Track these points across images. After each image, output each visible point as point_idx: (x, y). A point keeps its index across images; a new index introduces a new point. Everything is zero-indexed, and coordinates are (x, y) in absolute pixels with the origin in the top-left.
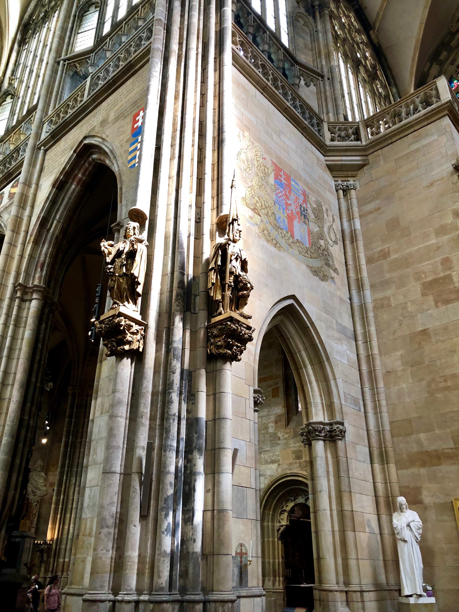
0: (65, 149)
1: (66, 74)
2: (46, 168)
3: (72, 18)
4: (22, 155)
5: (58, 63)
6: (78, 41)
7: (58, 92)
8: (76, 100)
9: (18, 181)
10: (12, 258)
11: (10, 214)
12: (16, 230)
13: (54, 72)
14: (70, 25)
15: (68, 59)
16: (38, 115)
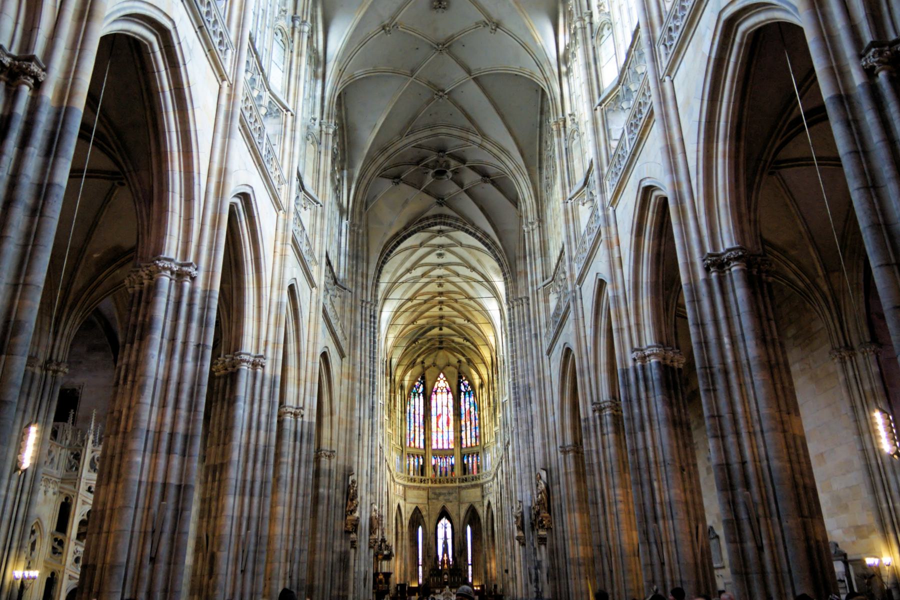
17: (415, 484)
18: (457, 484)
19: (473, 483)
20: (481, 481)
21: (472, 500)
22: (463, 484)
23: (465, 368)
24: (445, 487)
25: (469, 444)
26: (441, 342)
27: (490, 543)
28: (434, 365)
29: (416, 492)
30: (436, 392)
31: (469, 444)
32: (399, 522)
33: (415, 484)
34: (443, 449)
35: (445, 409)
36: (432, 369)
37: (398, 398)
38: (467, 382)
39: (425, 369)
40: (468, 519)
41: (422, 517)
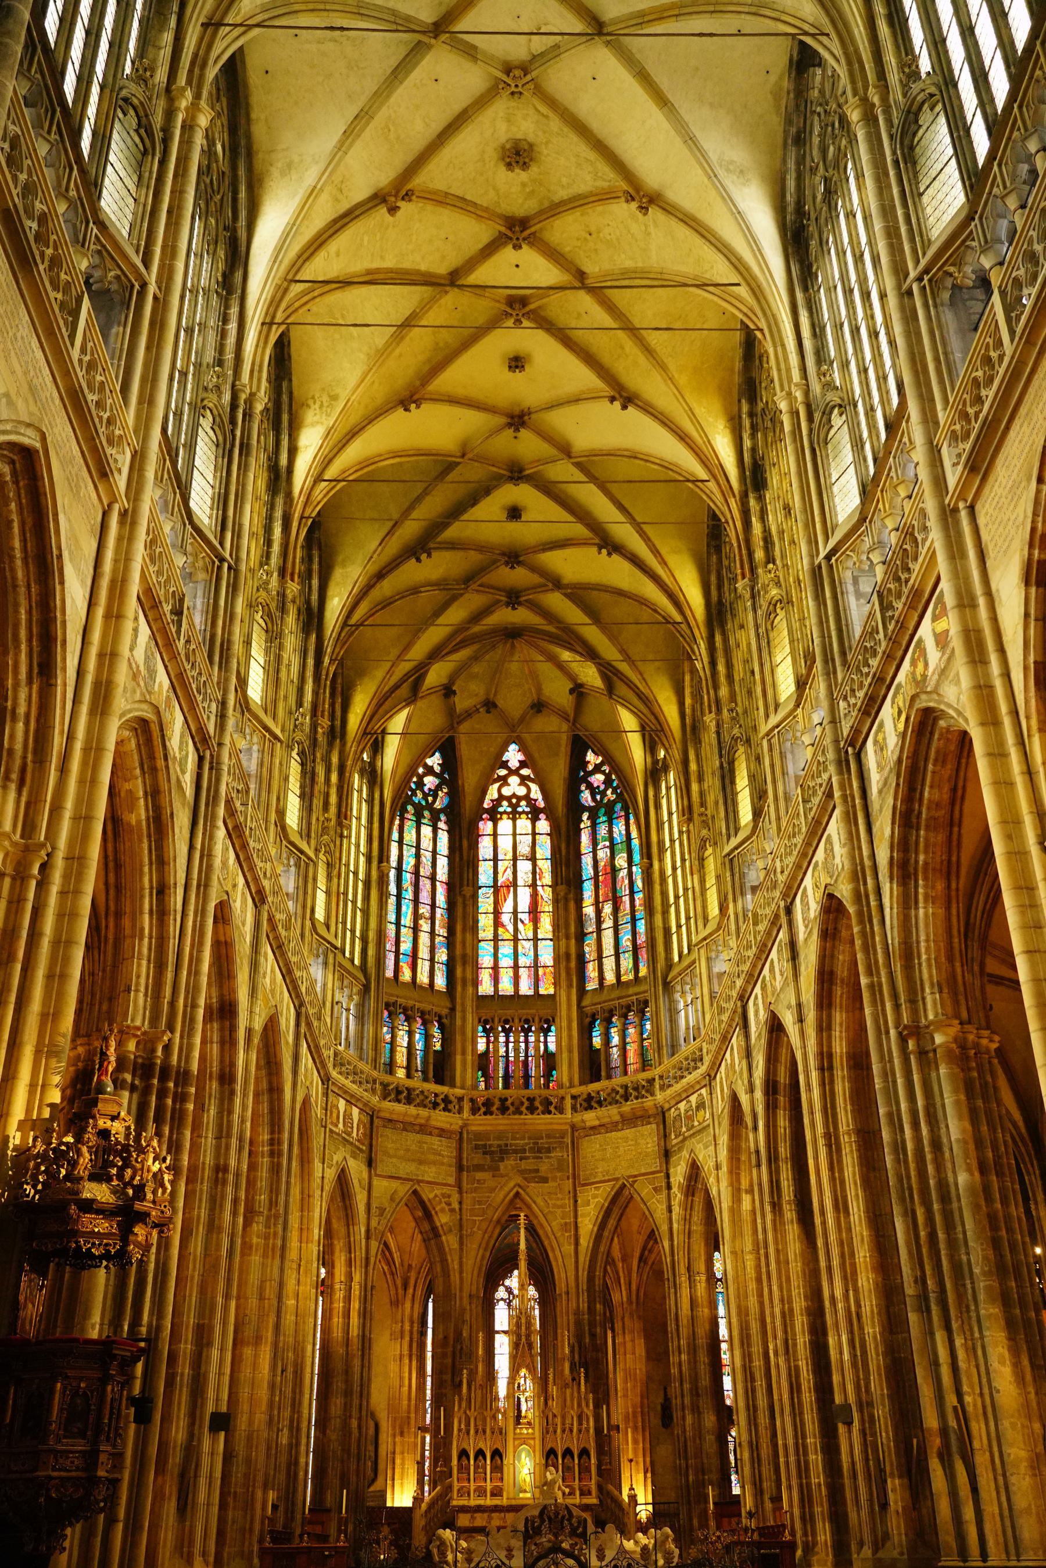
0: (1016, 485)
1: (936, 306)
2: (991, 547)
3: (892, 173)
4: (924, 540)
5: (910, 293)
6: (929, 210)
7: (937, 359)
8: (987, 361)
9: (941, 600)
10: (1010, 784)
11: (958, 682)
12: (991, 720)
13: (909, 318)
14: (895, 191)
15: (926, 271)
16: (915, 428)
17: (412, 1110)
20: (660, 1096)
21: (624, 1171)
23: (592, 720)
25: (610, 977)
26: (514, 598)
28: (490, 705)
29: (412, 1139)
30: (494, 815)
31: (610, 977)
34: (516, 996)
35: (524, 867)
36: (484, 722)
37: (359, 808)
38: (601, 777)
39: (454, 719)
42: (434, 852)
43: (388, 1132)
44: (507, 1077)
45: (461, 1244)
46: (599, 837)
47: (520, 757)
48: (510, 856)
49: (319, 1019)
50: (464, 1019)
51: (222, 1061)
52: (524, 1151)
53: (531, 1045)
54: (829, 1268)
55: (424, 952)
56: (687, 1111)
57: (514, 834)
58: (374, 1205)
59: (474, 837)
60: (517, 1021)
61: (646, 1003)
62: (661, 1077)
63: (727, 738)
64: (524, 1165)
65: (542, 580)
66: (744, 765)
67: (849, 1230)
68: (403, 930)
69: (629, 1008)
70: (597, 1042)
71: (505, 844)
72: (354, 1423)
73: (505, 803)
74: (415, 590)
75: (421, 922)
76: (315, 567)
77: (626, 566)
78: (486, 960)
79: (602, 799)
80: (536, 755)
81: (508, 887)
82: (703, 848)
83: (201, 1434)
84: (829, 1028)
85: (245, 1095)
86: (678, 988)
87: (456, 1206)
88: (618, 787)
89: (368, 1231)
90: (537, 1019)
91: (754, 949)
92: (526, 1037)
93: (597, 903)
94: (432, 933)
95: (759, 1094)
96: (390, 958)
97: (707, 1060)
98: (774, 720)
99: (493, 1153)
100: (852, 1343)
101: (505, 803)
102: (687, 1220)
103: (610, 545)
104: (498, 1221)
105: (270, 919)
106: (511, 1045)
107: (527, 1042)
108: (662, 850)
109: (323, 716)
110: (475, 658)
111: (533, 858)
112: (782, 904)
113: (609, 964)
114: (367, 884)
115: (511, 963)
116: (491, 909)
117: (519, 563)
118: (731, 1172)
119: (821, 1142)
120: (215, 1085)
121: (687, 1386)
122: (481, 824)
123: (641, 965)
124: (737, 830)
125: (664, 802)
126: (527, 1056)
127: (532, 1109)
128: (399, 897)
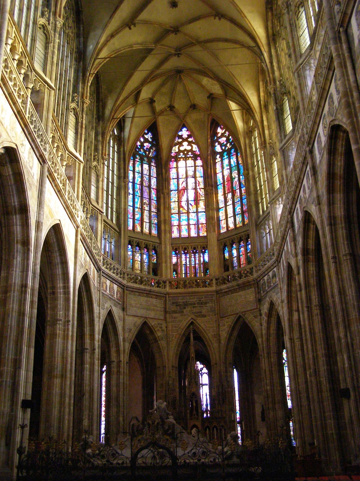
17: (142, 287)
18: (214, 288)
19: (241, 281)
20: (255, 275)
22: (224, 286)
24: (194, 292)
25: (231, 226)
26: (178, 52)
27: (276, 376)
28: (171, 108)
29: (143, 300)
30: (177, 159)
32: (113, 343)
33: (142, 287)
34: (189, 237)
35: (191, 181)
38: (224, 139)
40: (232, 344)
41: (156, 340)
42: (150, 176)
43: (132, 296)
44: (186, 273)
45: (168, 344)
46: (224, 165)
47: (187, 133)
48: (184, 176)
49: (91, 239)
50: (166, 247)
51: (23, 235)
52: (195, 304)
53: (197, 258)
54: (337, 323)
55: (146, 219)
56: (268, 280)
57: (186, 167)
58: (126, 328)
59: (168, 170)
60: (190, 248)
61: (248, 237)
62: (256, 267)
63: (278, 93)
64: (195, 310)
65: (191, 40)
66: (288, 105)
67: (346, 303)
68: (136, 210)
69: (240, 240)
70: (227, 255)
71: (182, 172)
72: (121, 419)
73: (182, 154)
74: (131, 46)
75: (144, 206)
76: (82, 32)
77: (228, 24)
78: (175, 222)
79: (225, 148)
80: (194, 130)
81: (184, 190)
82: (271, 159)
83: (17, 409)
84: (333, 204)
85: (36, 253)
86: (263, 227)
87: (164, 328)
88: (232, 141)
89: (124, 339)
90: (199, 247)
91: (295, 182)
92: (195, 255)
93: (225, 194)
94: (150, 211)
95: (300, 257)
96: (130, 222)
97: (276, 254)
98: (300, 62)
99: (182, 307)
100: (349, 358)
101: (182, 154)
102: (268, 328)
103: (220, 15)
104: (184, 334)
105: (51, 174)
106: (188, 260)
107: (195, 258)
108: (253, 166)
109: (86, 98)
110: (162, 85)
111: (194, 177)
112: (308, 149)
113: (231, 221)
114: (119, 189)
115: (186, 223)
116: (177, 200)
117: (178, 31)
118: (288, 302)
119: (331, 261)
120: (19, 246)
121: (270, 400)
122: (171, 163)
123: (246, 219)
124: (285, 136)
125: (253, 145)
126: (195, 264)
127: (198, 285)
128: (134, 195)
